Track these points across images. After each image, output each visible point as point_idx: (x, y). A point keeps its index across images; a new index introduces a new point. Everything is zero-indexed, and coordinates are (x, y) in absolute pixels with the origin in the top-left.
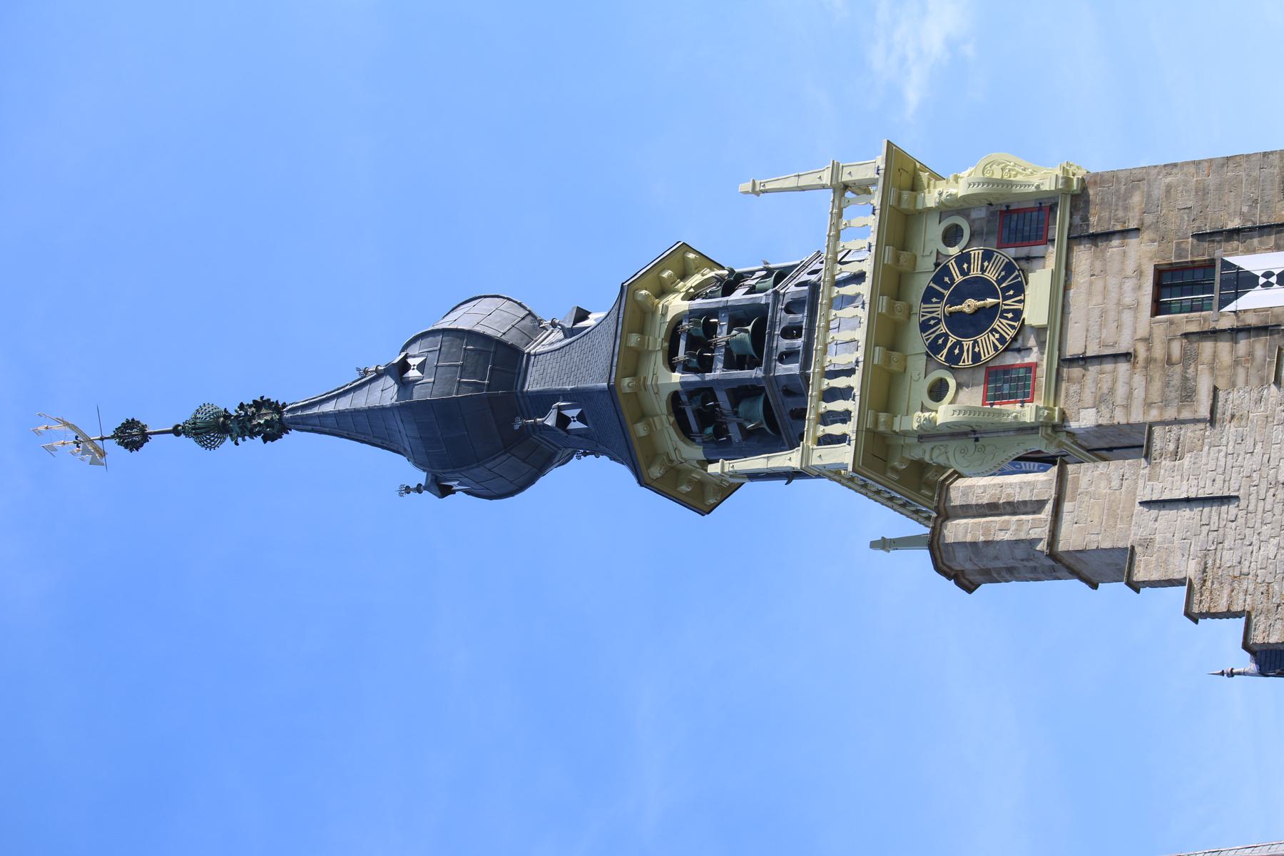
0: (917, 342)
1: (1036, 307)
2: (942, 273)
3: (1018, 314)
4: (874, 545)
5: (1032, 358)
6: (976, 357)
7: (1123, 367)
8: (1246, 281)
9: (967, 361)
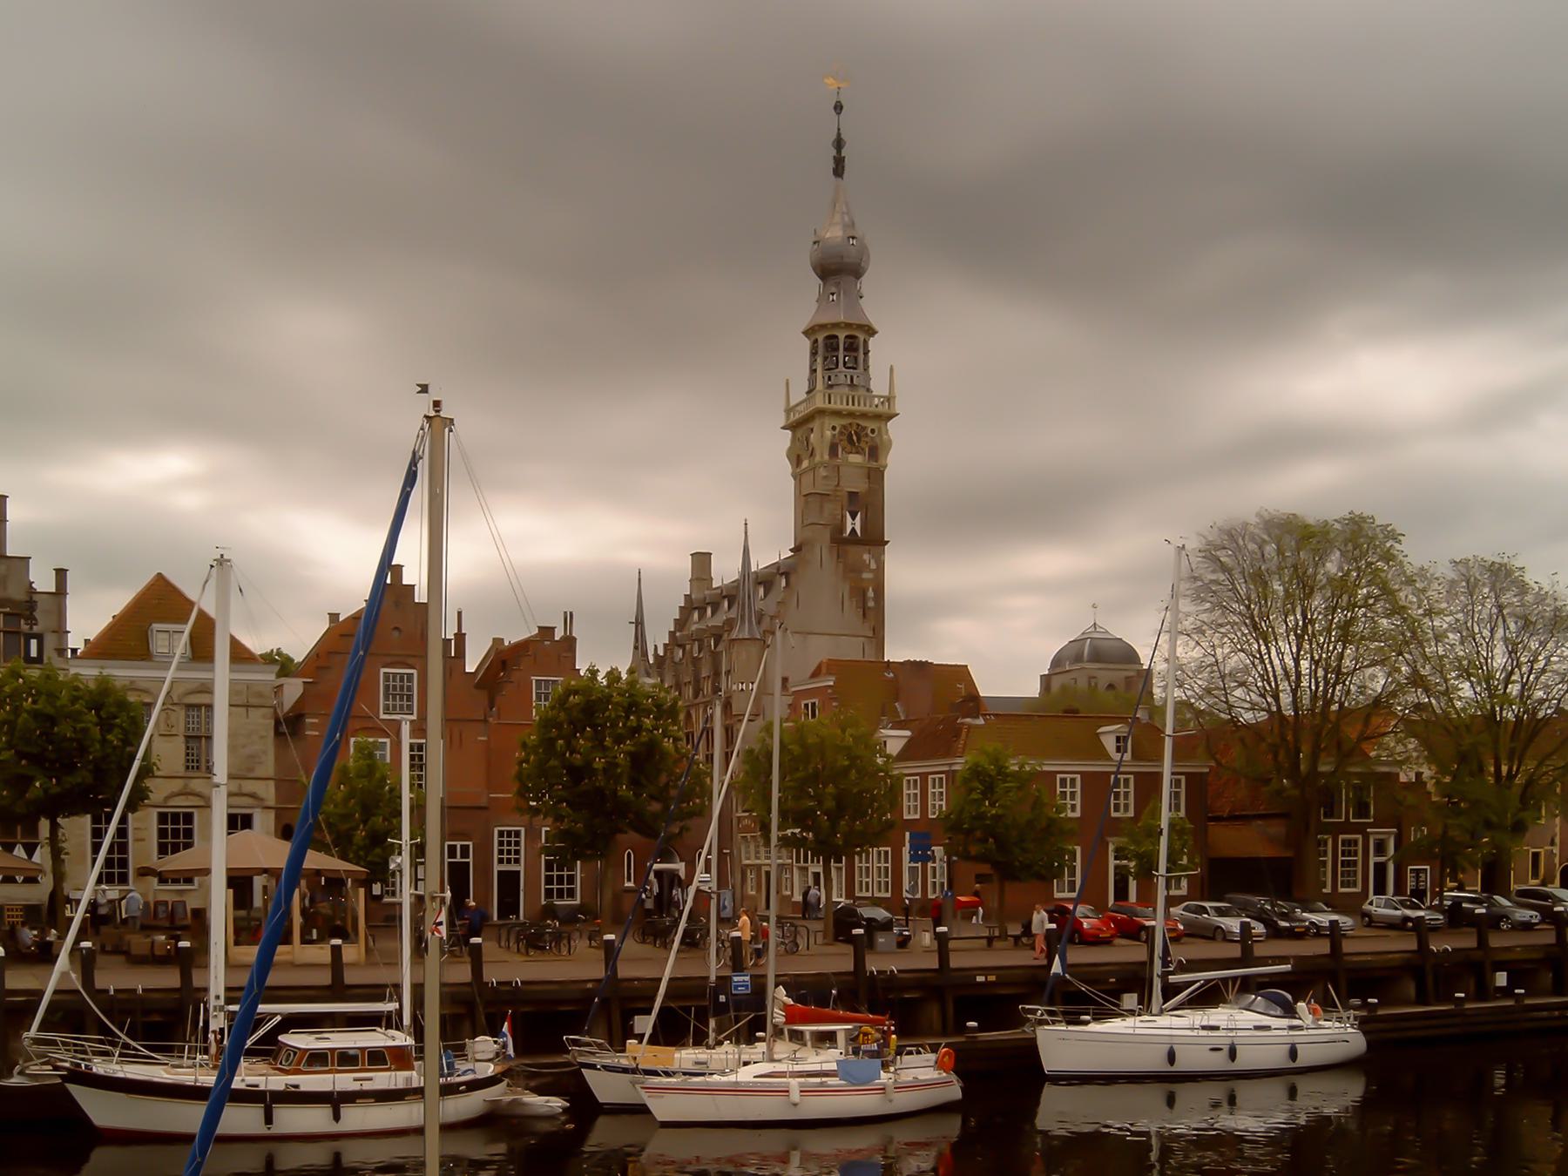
0: (845, 422)
1: (855, 458)
2: (864, 428)
3: (851, 453)
4: (787, 380)
5: (840, 456)
6: (841, 440)
7: (836, 483)
8: (853, 519)
9: (841, 437)
